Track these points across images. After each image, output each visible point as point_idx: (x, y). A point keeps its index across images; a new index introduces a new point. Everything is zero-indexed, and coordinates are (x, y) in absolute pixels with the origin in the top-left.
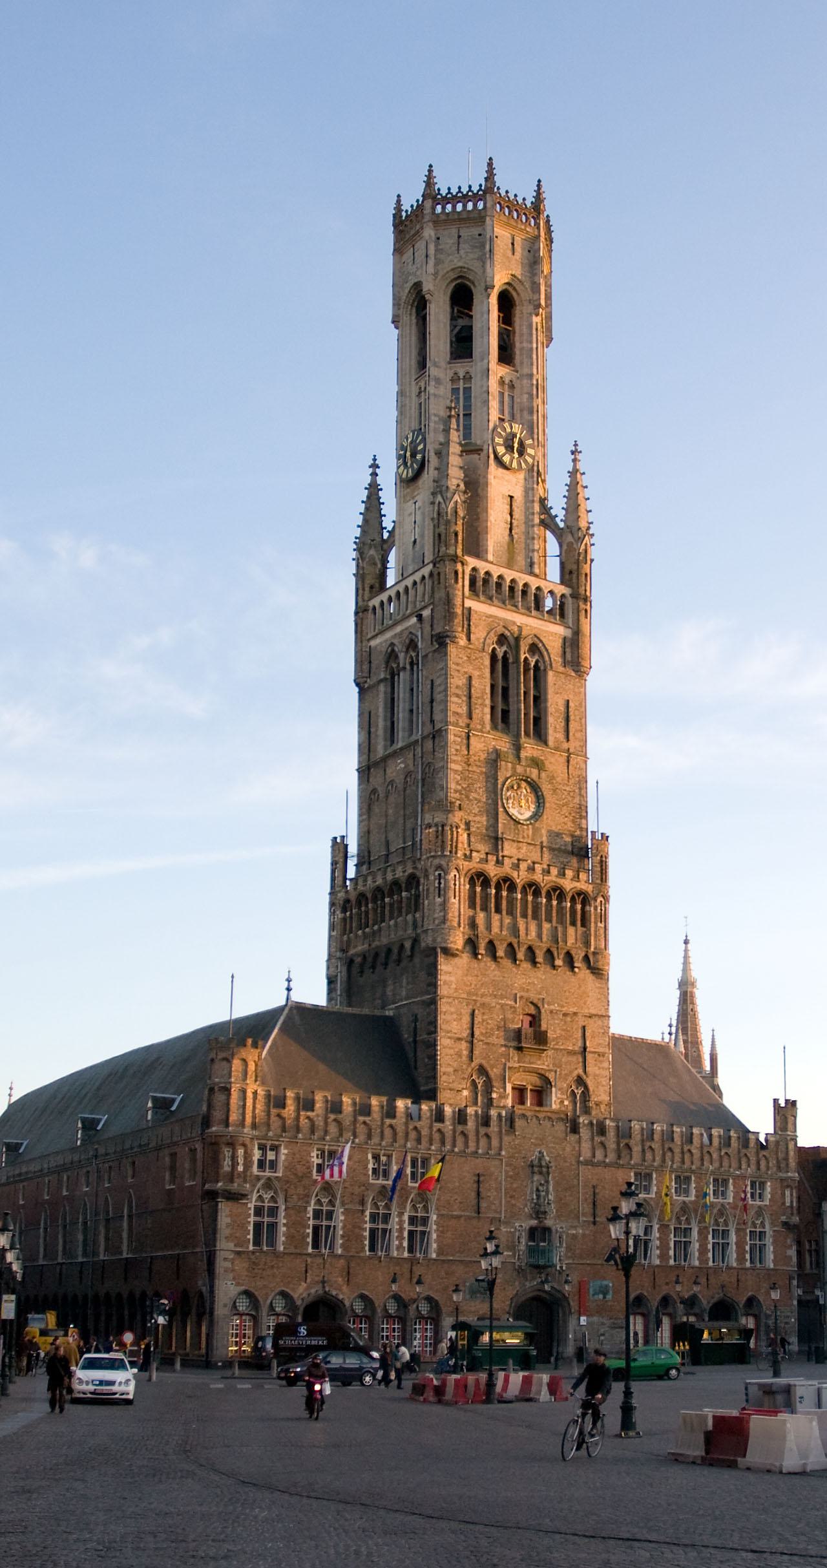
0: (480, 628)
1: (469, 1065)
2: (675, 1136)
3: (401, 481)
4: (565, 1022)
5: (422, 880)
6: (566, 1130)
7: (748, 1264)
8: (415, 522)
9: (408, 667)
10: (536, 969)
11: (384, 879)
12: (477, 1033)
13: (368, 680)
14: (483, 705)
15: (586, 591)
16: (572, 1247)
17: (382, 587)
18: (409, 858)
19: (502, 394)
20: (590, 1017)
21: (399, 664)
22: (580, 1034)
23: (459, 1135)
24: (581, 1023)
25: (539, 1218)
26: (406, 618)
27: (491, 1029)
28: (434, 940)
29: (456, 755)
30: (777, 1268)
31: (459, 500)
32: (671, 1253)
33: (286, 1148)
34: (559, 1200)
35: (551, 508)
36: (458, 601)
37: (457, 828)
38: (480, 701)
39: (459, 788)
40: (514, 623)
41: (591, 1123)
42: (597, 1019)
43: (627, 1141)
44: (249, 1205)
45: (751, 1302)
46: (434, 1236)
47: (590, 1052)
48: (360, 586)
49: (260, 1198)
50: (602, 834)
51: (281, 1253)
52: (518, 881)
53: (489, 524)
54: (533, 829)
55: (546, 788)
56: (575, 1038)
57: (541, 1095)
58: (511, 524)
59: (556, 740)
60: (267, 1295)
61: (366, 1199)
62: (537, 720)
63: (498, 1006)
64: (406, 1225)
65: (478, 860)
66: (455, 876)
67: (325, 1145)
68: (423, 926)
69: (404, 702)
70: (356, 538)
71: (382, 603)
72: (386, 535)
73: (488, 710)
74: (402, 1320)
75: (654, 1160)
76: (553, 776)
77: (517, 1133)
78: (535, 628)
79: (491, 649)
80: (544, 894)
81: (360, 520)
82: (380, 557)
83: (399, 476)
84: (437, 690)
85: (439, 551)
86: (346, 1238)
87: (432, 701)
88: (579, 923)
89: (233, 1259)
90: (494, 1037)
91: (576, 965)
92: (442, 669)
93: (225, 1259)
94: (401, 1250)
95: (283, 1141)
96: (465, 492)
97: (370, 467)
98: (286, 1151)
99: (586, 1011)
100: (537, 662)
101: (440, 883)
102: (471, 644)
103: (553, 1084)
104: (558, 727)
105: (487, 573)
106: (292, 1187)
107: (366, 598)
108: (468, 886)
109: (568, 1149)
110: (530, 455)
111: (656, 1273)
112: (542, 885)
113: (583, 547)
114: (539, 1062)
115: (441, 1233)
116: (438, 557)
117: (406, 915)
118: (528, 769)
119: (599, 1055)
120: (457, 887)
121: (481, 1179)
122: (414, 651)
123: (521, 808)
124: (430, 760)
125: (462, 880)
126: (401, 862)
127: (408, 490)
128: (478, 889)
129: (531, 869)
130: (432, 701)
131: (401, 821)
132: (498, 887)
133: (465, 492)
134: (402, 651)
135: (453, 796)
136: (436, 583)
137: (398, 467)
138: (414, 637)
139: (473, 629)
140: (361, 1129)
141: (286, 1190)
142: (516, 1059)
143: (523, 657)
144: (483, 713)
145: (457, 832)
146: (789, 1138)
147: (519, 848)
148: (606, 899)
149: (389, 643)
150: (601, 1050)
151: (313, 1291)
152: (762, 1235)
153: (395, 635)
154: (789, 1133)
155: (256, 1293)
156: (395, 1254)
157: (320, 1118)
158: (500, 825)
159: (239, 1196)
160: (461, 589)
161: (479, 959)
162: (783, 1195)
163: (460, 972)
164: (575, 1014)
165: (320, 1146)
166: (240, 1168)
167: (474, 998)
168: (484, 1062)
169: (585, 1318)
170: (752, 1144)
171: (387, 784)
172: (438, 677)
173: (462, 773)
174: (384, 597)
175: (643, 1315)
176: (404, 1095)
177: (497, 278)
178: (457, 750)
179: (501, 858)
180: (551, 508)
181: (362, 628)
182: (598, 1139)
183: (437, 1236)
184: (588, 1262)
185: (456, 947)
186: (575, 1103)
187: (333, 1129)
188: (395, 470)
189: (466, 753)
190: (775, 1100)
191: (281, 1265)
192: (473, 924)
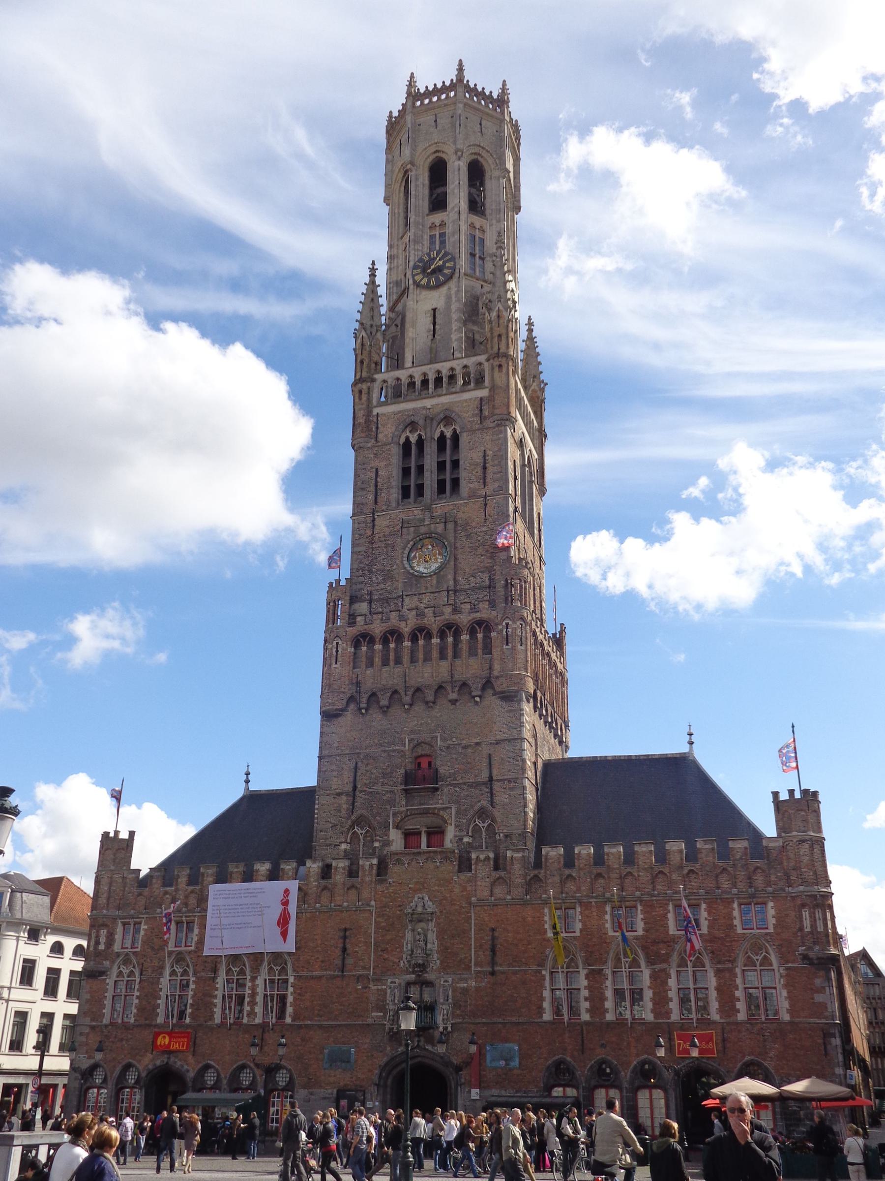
0: (389, 426)
7: (742, 1016)
10: (430, 709)
12: (359, 785)
15: (499, 349)
16: (462, 1004)
20: (497, 744)
22: (485, 764)
23: (323, 890)
25: (417, 971)
29: (360, 539)
30: (797, 1020)
31: (365, 335)
33: (146, 924)
34: (444, 950)
39: (362, 565)
40: (424, 408)
41: (488, 858)
43: (536, 872)
44: (108, 981)
47: (498, 780)
49: (120, 974)
53: (407, 340)
54: (437, 578)
60: (114, 1067)
61: (219, 965)
62: (456, 482)
64: (260, 990)
67: (182, 917)
75: (579, 890)
76: (467, 524)
78: (447, 403)
80: (435, 633)
86: (195, 1007)
88: (480, 652)
89: (88, 1034)
93: (81, 1034)
94: (252, 1016)
98: (146, 927)
100: (455, 431)
102: (378, 442)
103: (448, 822)
104: (473, 477)
105: (398, 379)
106: (149, 960)
109: (457, 890)
110: (448, 268)
111: (585, 1032)
113: (494, 314)
115: (299, 994)
118: (432, 525)
119: (509, 782)
121: (348, 933)
125: (344, 645)
129: (420, 615)
132: (385, 641)
141: (143, 964)
142: (404, 803)
147: (420, 600)
151: (158, 1063)
154: (795, 833)
157: (180, 892)
160: (365, 403)
161: (362, 714)
164: (478, 744)
166: (102, 947)
167: (358, 751)
168: (364, 812)
169: (478, 1091)
176: (261, 859)
178: (360, 535)
183: (295, 999)
184: (484, 1020)
185: (335, 707)
191: (130, 1036)
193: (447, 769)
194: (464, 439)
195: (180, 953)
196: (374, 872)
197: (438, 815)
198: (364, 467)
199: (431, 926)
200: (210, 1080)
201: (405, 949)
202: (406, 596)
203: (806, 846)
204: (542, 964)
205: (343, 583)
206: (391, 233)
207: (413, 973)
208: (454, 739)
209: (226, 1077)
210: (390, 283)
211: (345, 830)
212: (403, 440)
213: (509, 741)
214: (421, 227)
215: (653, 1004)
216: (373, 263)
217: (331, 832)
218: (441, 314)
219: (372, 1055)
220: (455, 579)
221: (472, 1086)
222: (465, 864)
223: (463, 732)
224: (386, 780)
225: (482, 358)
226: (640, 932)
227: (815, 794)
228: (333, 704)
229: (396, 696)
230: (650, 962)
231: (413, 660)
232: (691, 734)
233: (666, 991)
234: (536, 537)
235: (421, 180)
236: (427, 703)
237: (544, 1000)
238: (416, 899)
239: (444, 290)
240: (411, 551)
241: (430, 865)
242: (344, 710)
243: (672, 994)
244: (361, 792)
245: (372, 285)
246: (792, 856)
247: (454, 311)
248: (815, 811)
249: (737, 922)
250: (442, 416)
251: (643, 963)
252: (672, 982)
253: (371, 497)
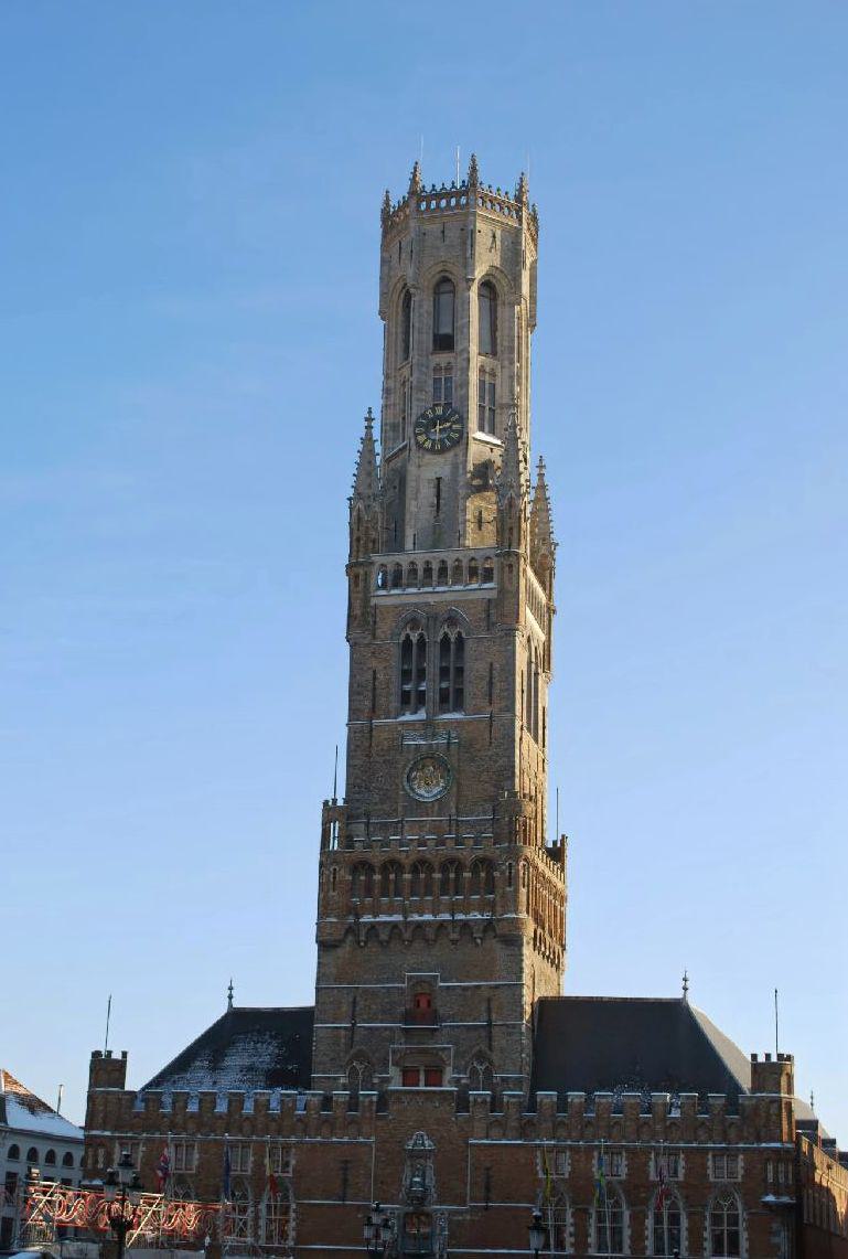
1: (347, 1052)
39: (358, 781)
40: (427, 604)
53: (408, 517)
57: (434, 1076)
62: (460, 692)
76: (471, 745)
80: (436, 865)
100: (459, 633)
105: (398, 564)
109: (455, 1129)
121: (349, 1165)
125: (342, 872)
139: (379, 624)
142: (403, 1040)
152: (734, 1220)
158: (400, 809)
161: (362, 947)
162: (766, 1170)
189: (367, 745)
194: (470, 646)
195: (181, 1175)
197: (437, 1054)
199: (430, 1163)
201: (403, 1183)
205: (340, 803)
206: (388, 359)
210: (386, 424)
212: (403, 638)
214: (424, 369)
216: (370, 412)
220: (457, 808)
226: (624, 1177)
227: (789, 1058)
228: (331, 934)
229: (396, 931)
230: (631, 1204)
232: (685, 980)
233: (643, 1231)
234: (540, 739)
235: (425, 307)
236: (427, 941)
238: (414, 1137)
239: (450, 455)
240: (412, 770)
242: (342, 941)
243: (649, 1233)
245: (368, 440)
246: (763, 1115)
247: (461, 483)
248: (787, 1074)
249: (710, 1172)
250: (446, 616)
251: (624, 1207)
252: (650, 1222)
253: (368, 703)
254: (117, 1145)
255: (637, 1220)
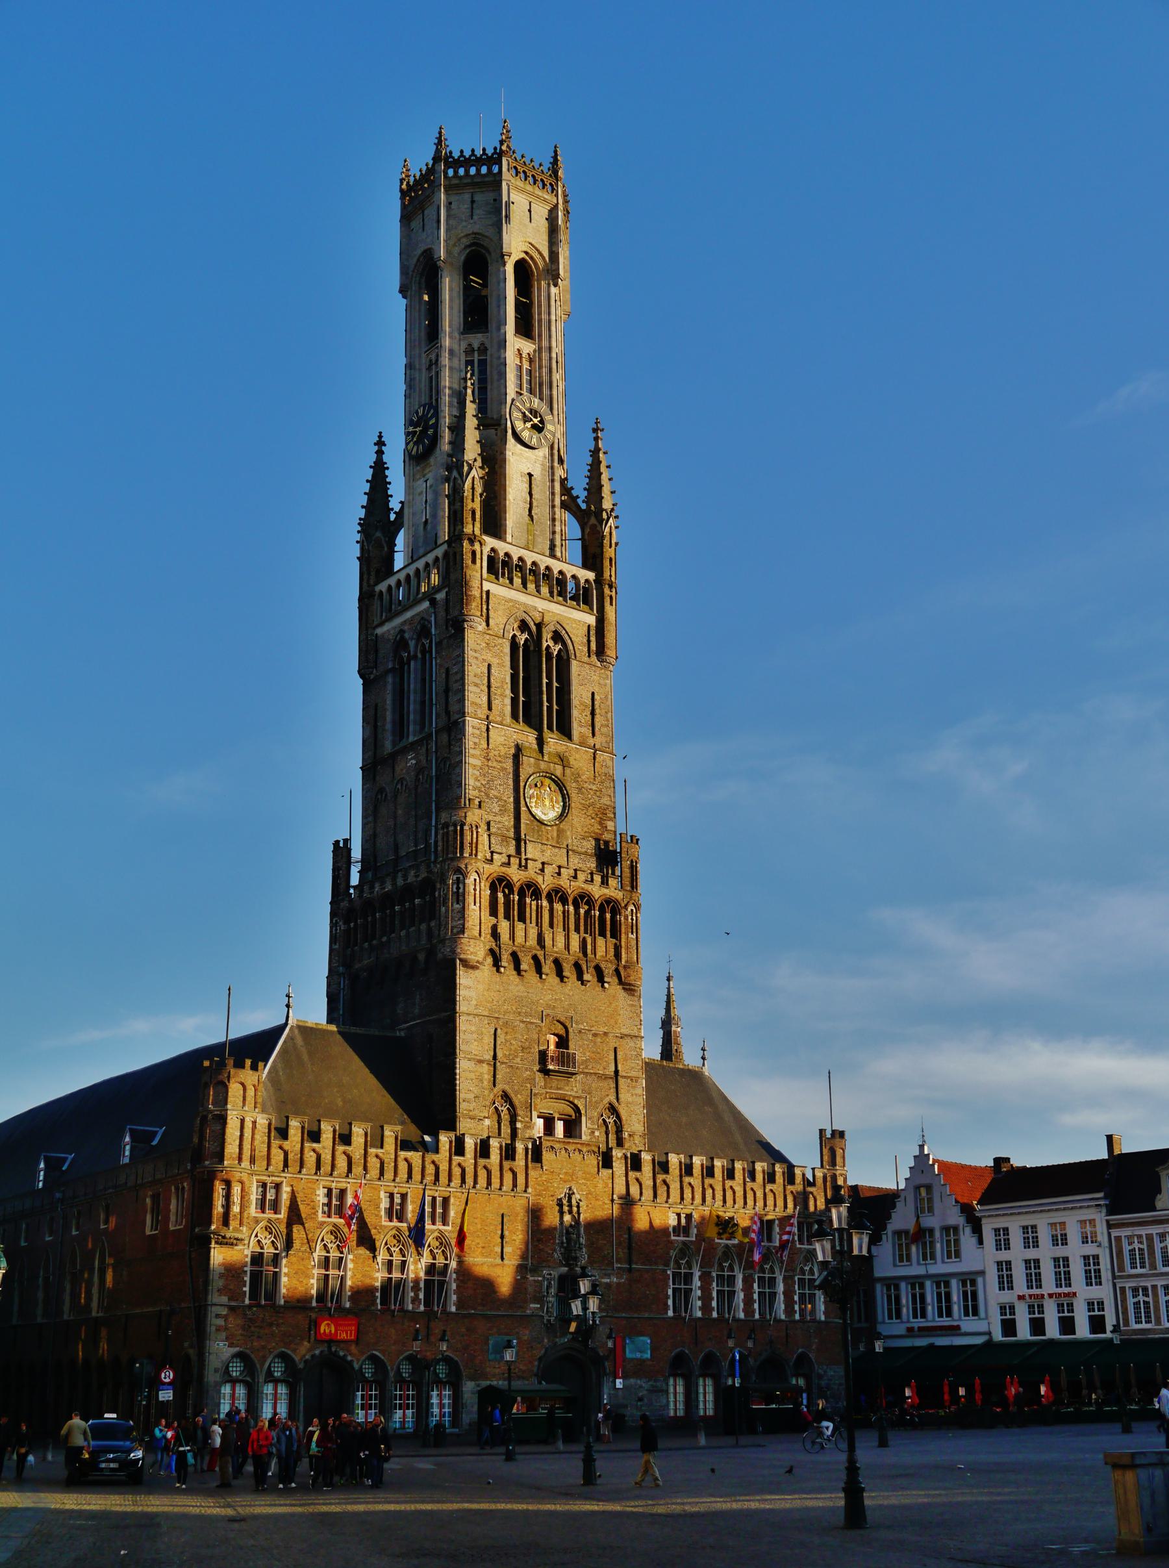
0: (500, 613)
2: (716, 1170)
3: (410, 460)
4: (595, 1043)
5: (438, 886)
6: (598, 1163)
8: (426, 501)
9: (419, 655)
11: (394, 884)
12: (500, 1055)
13: (375, 671)
14: (503, 695)
15: (611, 576)
17: (388, 570)
18: (422, 862)
19: (520, 368)
20: (621, 1038)
21: (409, 653)
22: (612, 1057)
24: (612, 1045)
26: (418, 602)
27: (514, 1051)
28: (454, 952)
30: (829, 1320)
31: (476, 476)
32: (714, 1304)
35: (572, 488)
36: (475, 583)
37: (477, 827)
38: (499, 692)
39: (478, 784)
40: (535, 608)
42: (628, 1040)
45: (803, 1360)
46: (454, 1286)
47: (622, 1077)
48: (365, 569)
50: (632, 837)
51: (280, 1306)
52: (543, 887)
53: (507, 502)
54: (558, 831)
55: (571, 787)
56: (606, 1062)
58: (531, 503)
59: (582, 735)
60: (264, 1359)
63: (522, 1025)
65: (500, 864)
66: (475, 880)
67: (333, 1182)
68: (439, 935)
69: (415, 692)
70: (360, 519)
71: (390, 587)
72: (393, 517)
73: (508, 701)
74: (418, 1386)
75: (693, 1198)
76: (579, 776)
77: (545, 1168)
79: (511, 635)
81: (364, 500)
82: (387, 539)
83: (408, 453)
84: (453, 679)
85: (455, 530)
87: (447, 690)
88: (608, 934)
90: (519, 1059)
91: (606, 979)
92: (458, 656)
93: (218, 1316)
94: (417, 1303)
95: (286, 1178)
96: (482, 468)
97: (375, 444)
99: (617, 1031)
101: (458, 888)
103: (583, 1112)
107: (372, 582)
108: (489, 892)
109: (600, 1185)
110: (550, 431)
112: (570, 892)
114: (567, 1088)
116: (454, 535)
117: (420, 924)
118: (552, 765)
119: (632, 1080)
120: (478, 892)
122: (426, 638)
123: (546, 808)
124: (446, 755)
126: (413, 865)
127: (418, 468)
128: (500, 895)
130: (447, 690)
131: (412, 821)
132: (522, 894)
133: (482, 468)
134: (412, 639)
135: (471, 793)
136: (451, 564)
137: (407, 444)
138: (426, 623)
139: (491, 614)
140: (373, 1163)
143: (545, 645)
144: (503, 703)
145: (477, 832)
146: (838, 1173)
147: (543, 851)
148: (638, 907)
149: (398, 629)
150: (633, 1074)
151: (317, 1352)
153: (405, 621)
155: (253, 1356)
156: (410, 1307)
157: (326, 1151)
158: (522, 825)
159: (235, 1241)
163: (481, 987)
164: (606, 1034)
165: (328, 1184)
167: (496, 1015)
168: (507, 1088)
169: (621, 1380)
170: (798, 1179)
171: (395, 782)
172: (454, 665)
173: (481, 769)
174: (392, 581)
175: (683, 1376)
177: (514, 244)
179: (523, 863)
180: (572, 488)
181: (367, 615)
182: (632, 1174)
183: (457, 1287)
184: (624, 1315)
185: (477, 958)
186: (607, 1134)
187: (342, 1163)
188: (404, 446)
189: (486, 746)
190: (821, 1131)
191: (281, 1321)
192: (495, 934)
193: (580, 1055)
196: (530, 1156)
198: (476, 655)
200: (368, 1373)
201: (557, 1241)
202: (529, 841)
203: (842, 1179)
204: (667, 1264)
207: (565, 1266)
208: (585, 1024)
209: (392, 1369)
211: (488, 1103)
213: (632, 1037)
215: (744, 1305)
217: (474, 1104)
218: (538, 487)
219: (532, 1347)
221: (616, 1377)
222: (607, 1161)
223: (593, 1018)
224: (526, 1056)
225: (591, 576)
227: (842, 1134)
228: (475, 954)
231: (551, 925)
232: (703, 1049)
233: (752, 1294)
237: (669, 1298)
241: (577, 1156)
244: (503, 1063)
252: (756, 1286)
253: (485, 699)
254: (255, 1183)
255: (748, 1282)
